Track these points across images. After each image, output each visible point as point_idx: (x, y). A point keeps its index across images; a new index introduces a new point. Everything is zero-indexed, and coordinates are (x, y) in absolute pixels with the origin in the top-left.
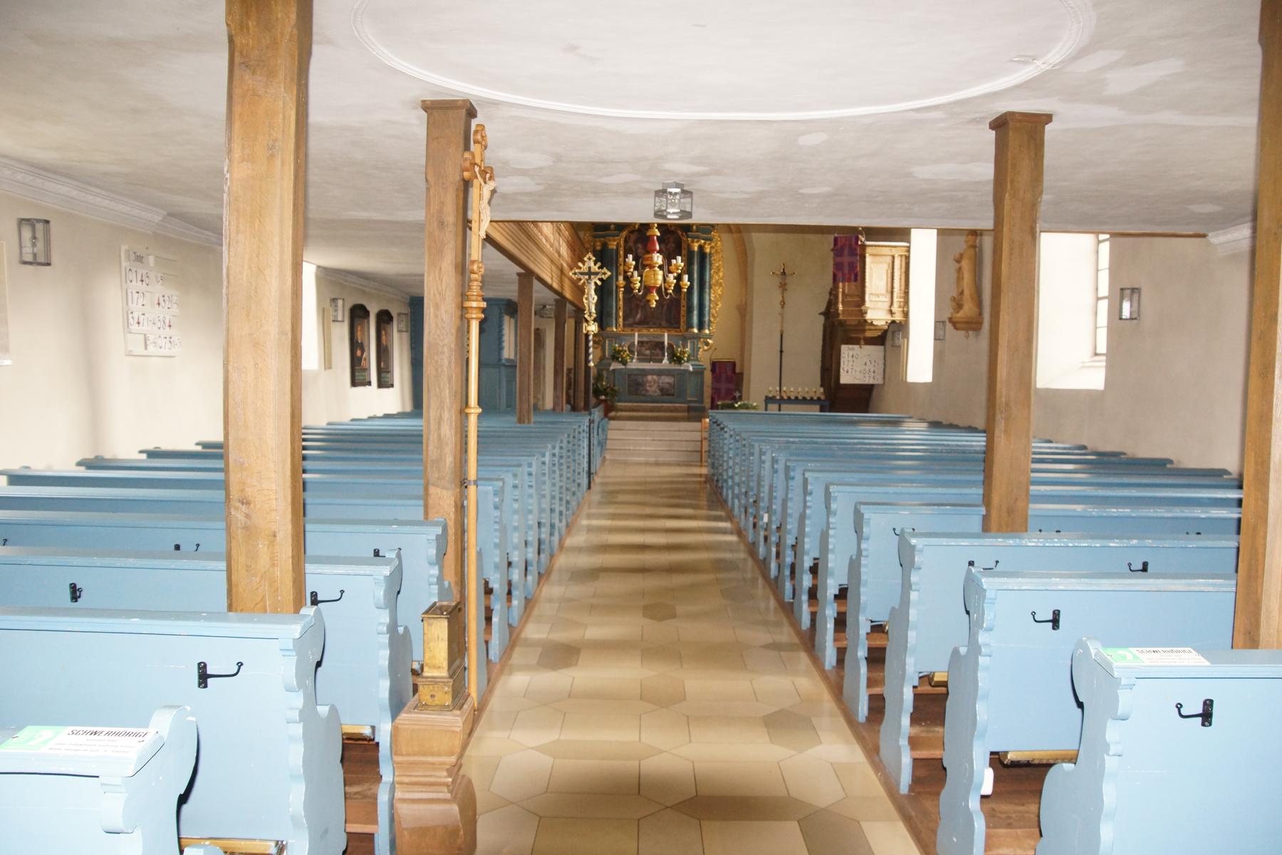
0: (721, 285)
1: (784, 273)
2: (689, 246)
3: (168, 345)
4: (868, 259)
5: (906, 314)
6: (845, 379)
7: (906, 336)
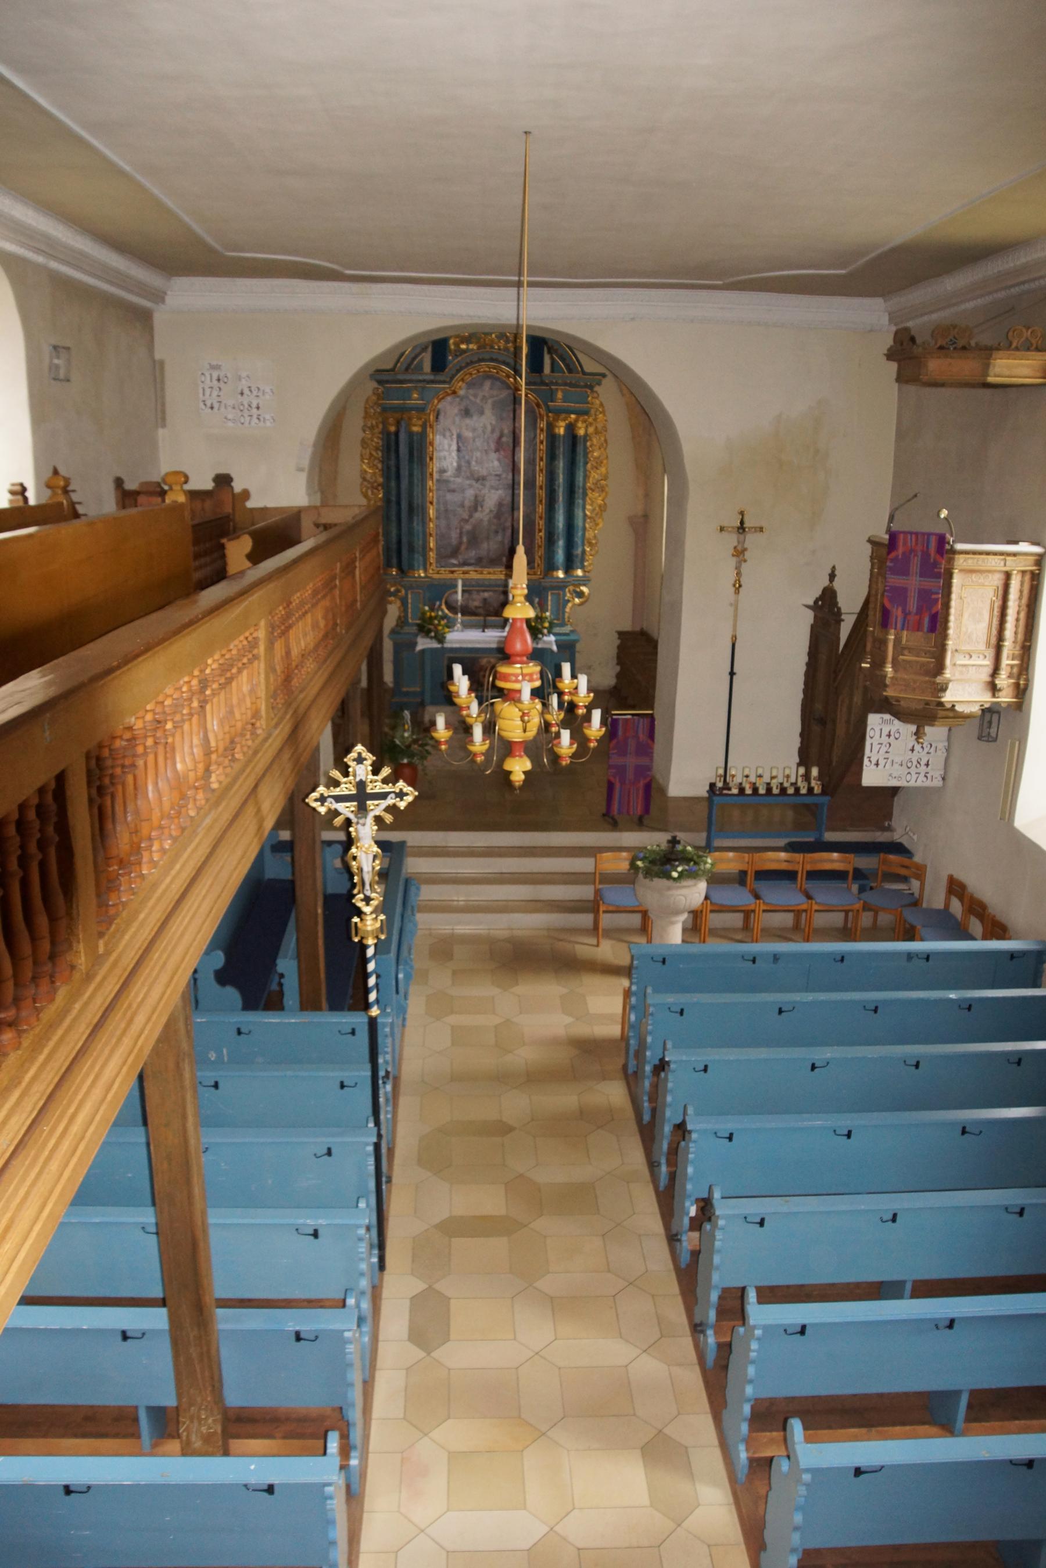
0: (602, 489)
1: (742, 528)
4: (957, 580)
5: (1022, 691)
6: (872, 777)
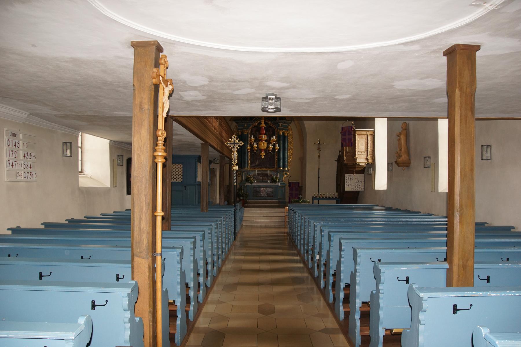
2: (278, 133)
3: (30, 176)
4: (357, 137)
5: (374, 160)
6: (347, 189)
7: (374, 169)
